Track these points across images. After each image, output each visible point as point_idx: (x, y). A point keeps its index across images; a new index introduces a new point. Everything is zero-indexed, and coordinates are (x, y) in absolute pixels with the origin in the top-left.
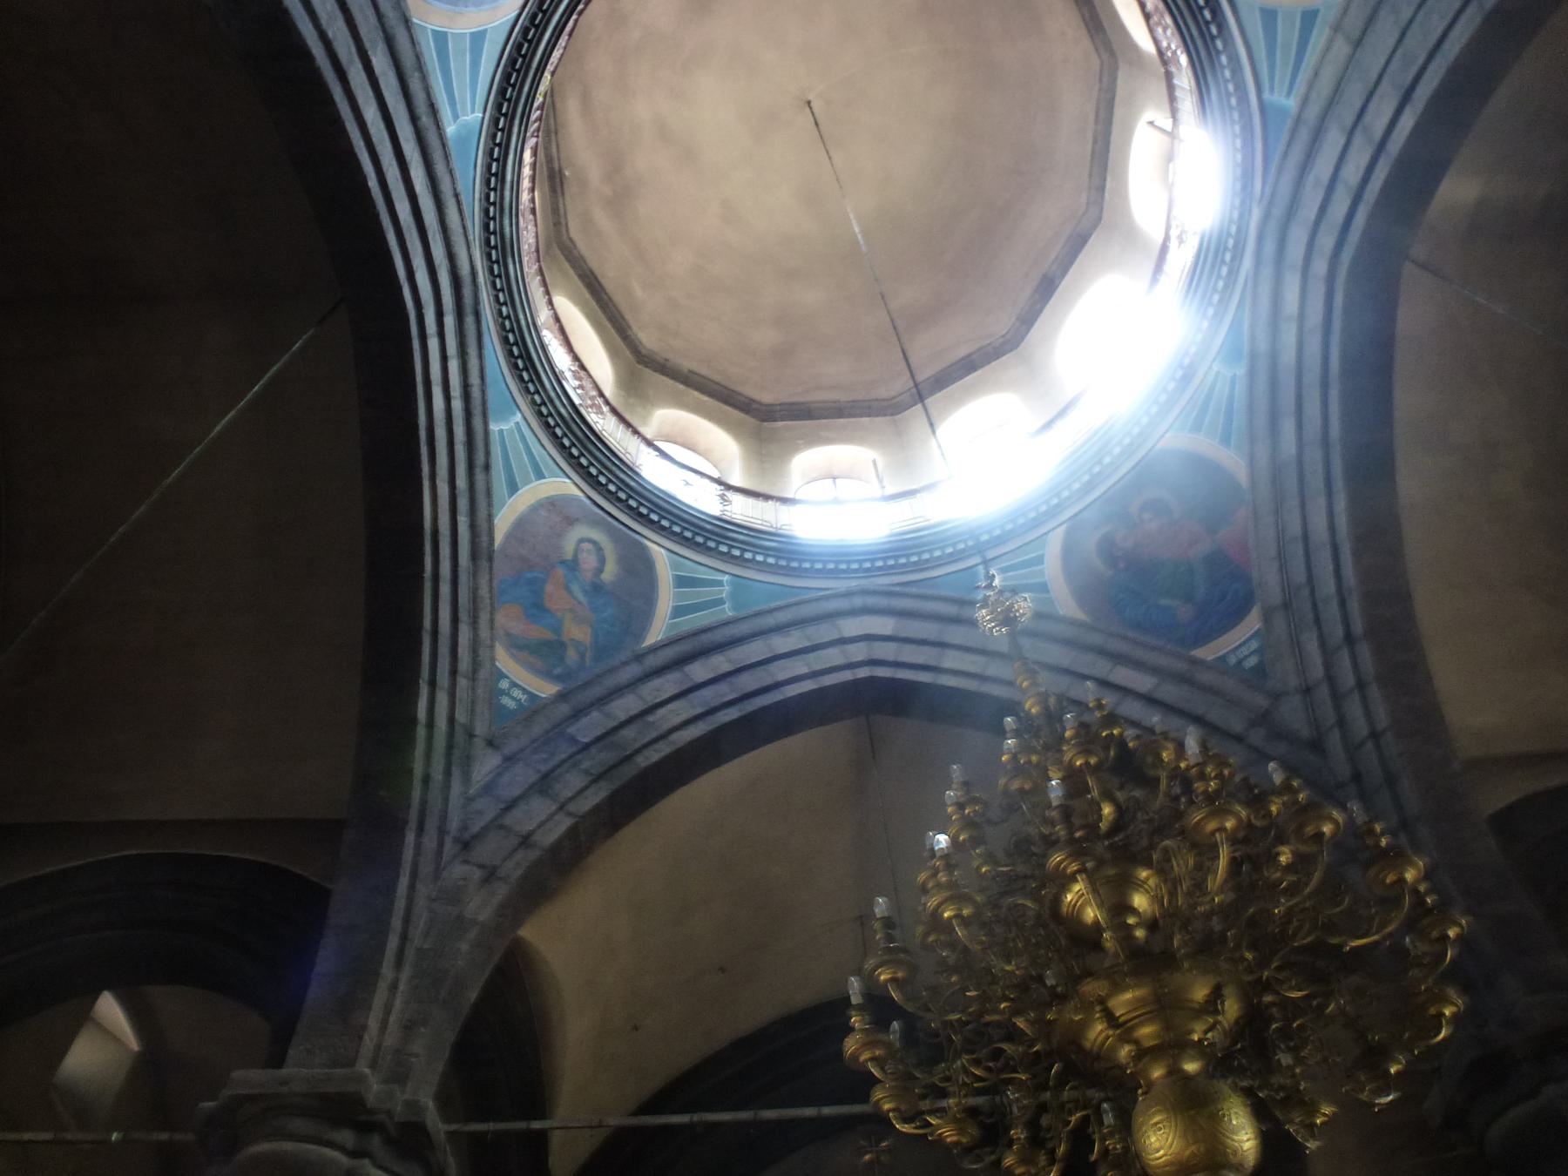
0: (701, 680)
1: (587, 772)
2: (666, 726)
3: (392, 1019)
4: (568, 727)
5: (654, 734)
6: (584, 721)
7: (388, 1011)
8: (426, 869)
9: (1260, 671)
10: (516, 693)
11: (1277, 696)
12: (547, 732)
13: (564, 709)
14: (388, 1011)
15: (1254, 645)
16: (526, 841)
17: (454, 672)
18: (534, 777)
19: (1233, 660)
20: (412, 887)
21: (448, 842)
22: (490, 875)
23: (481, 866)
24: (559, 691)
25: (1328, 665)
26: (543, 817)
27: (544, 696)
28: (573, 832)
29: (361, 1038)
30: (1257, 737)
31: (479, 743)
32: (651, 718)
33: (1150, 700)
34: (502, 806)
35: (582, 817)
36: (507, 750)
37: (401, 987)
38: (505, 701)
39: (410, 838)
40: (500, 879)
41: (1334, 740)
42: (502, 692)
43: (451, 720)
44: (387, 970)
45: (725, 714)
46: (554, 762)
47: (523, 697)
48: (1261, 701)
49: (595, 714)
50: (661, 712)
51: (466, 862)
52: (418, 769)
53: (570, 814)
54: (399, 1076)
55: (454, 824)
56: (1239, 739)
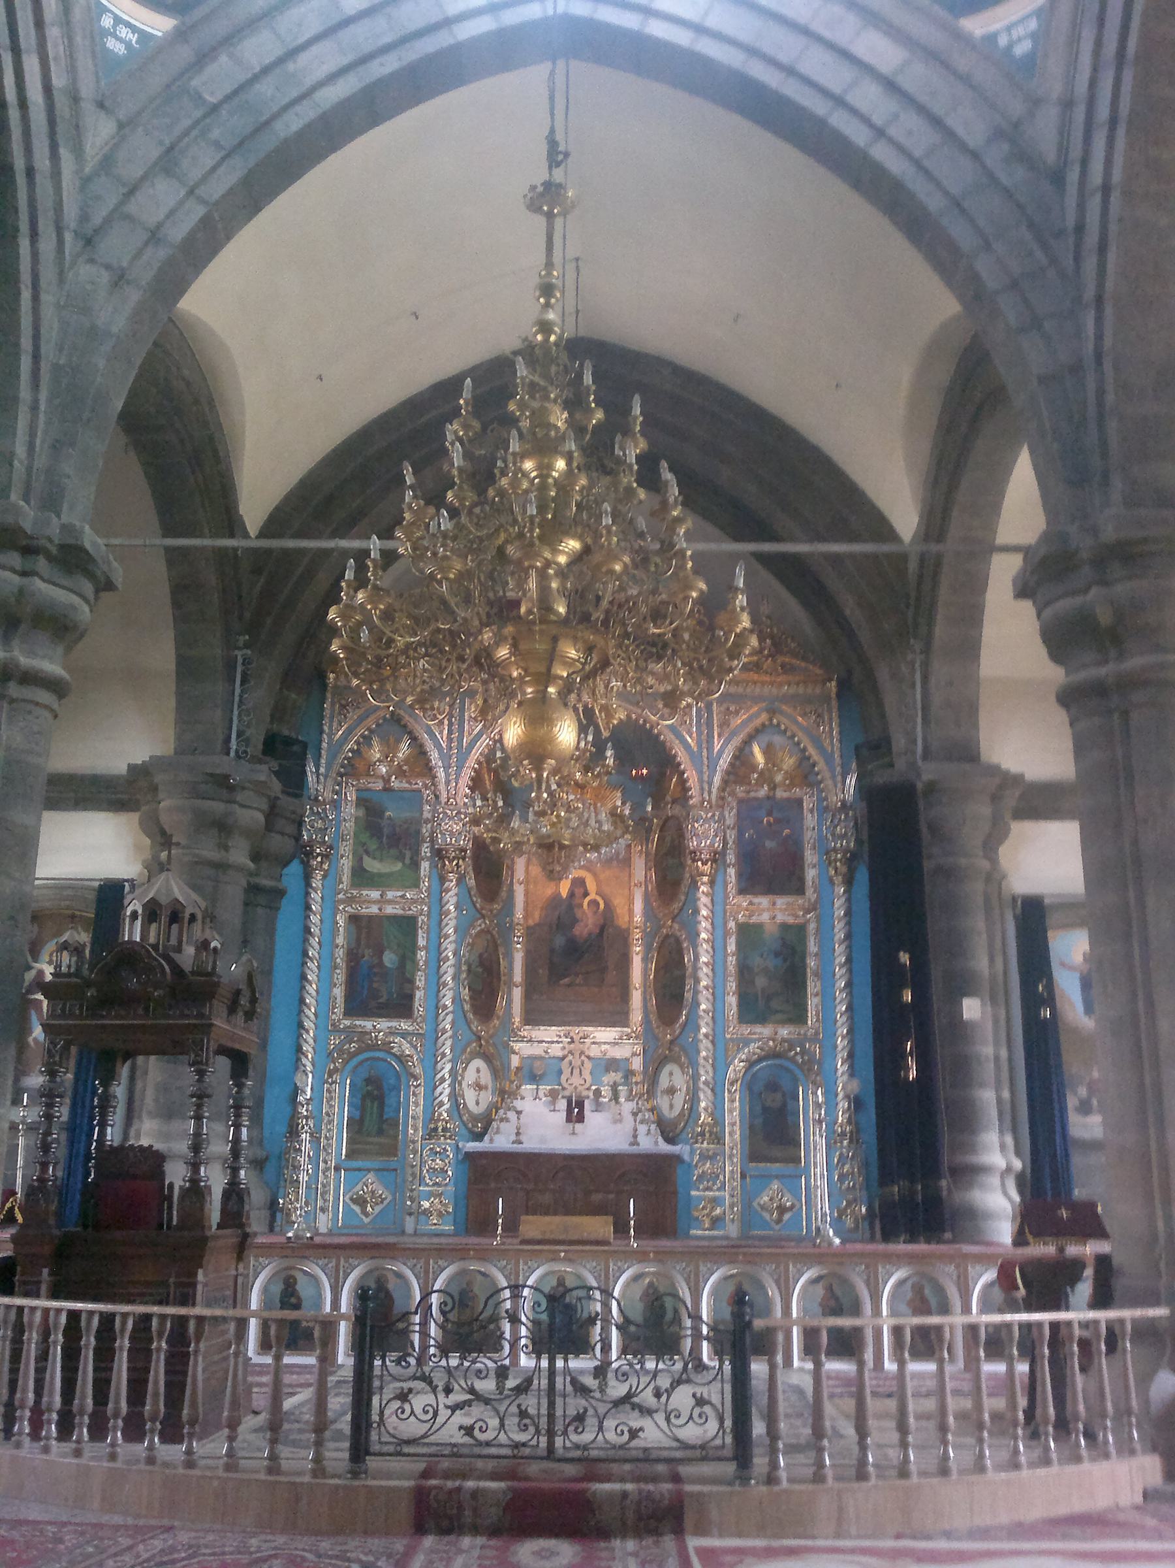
0: (352, 12)
1: (217, 144)
2: (309, 82)
3: (38, 442)
4: (191, 78)
5: (294, 93)
6: (211, 69)
7: (32, 435)
8: (48, 275)
9: (1029, 64)
10: (123, 32)
11: (1036, 102)
12: (168, 86)
13: (185, 53)
14: (32, 435)
15: (1033, 25)
16: (154, 236)
17: (39, 24)
18: (155, 153)
19: (1003, 41)
20: (36, 298)
21: (68, 237)
22: (120, 279)
23: (108, 267)
24: (175, 27)
25: (1093, 84)
26: (172, 204)
27: (160, 34)
28: (206, 222)
29: (11, 465)
30: (994, 157)
31: (87, 106)
32: (291, 66)
33: (890, 85)
34: (125, 190)
35: (217, 203)
36: (122, 114)
37: (42, 407)
38: (111, 44)
39: (24, 244)
40: (128, 283)
41: (1073, 176)
42: (105, 33)
43: (48, 89)
44: (25, 393)
45: (382, 65)
46: (178, 130)
47: (134, 39)
48: (1016, 107)
49: (223, 59)
50: (303, 58)
51: (91, 261)
52: (19, 164)
53: (202, 201)
54: (52, 502)
55: (71, 212)
56: (975, 155)
